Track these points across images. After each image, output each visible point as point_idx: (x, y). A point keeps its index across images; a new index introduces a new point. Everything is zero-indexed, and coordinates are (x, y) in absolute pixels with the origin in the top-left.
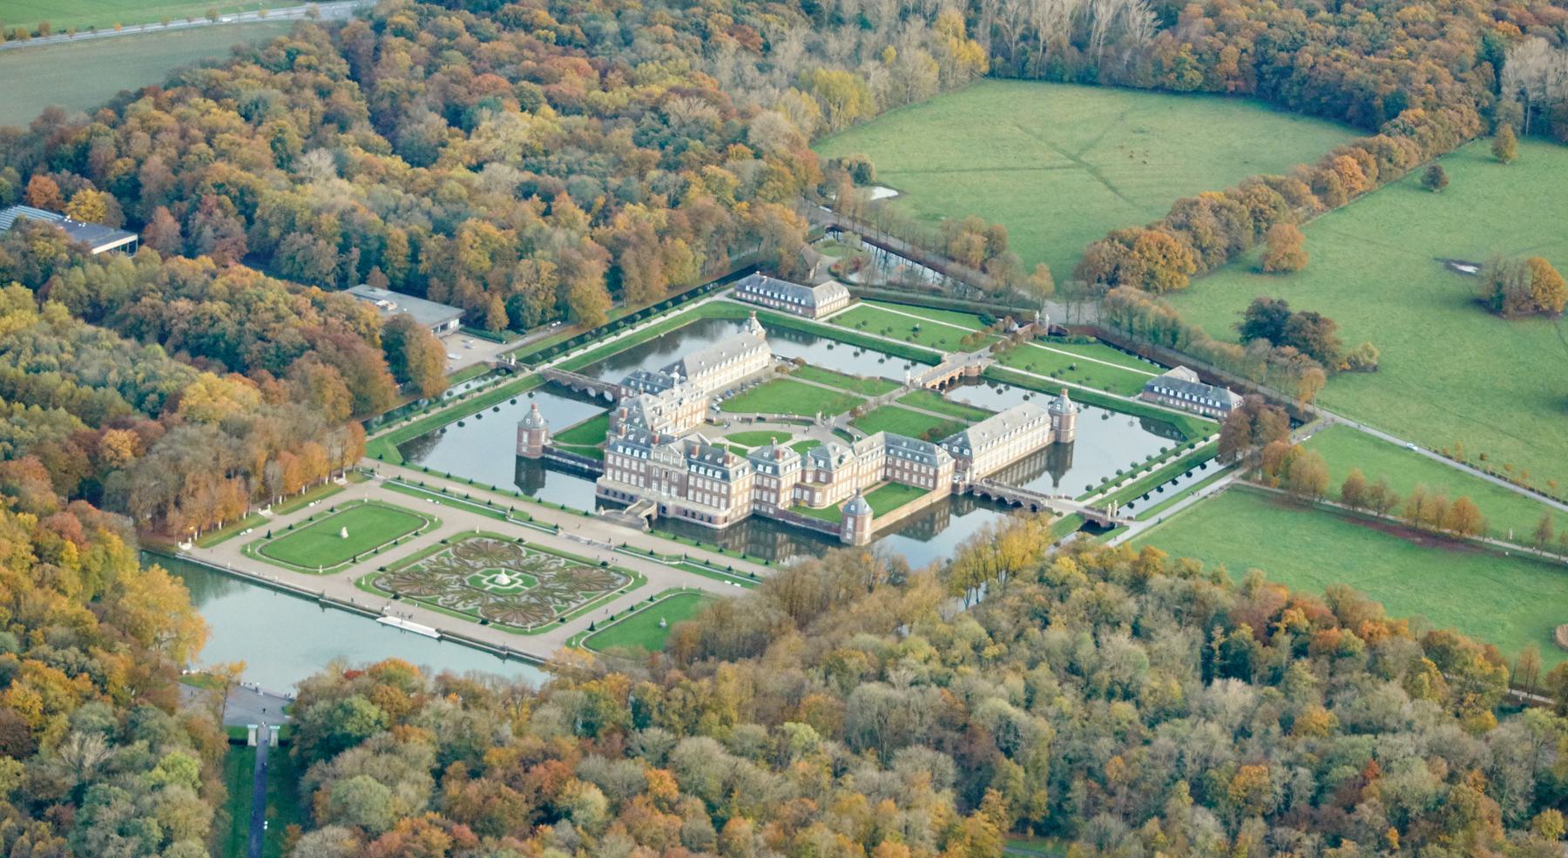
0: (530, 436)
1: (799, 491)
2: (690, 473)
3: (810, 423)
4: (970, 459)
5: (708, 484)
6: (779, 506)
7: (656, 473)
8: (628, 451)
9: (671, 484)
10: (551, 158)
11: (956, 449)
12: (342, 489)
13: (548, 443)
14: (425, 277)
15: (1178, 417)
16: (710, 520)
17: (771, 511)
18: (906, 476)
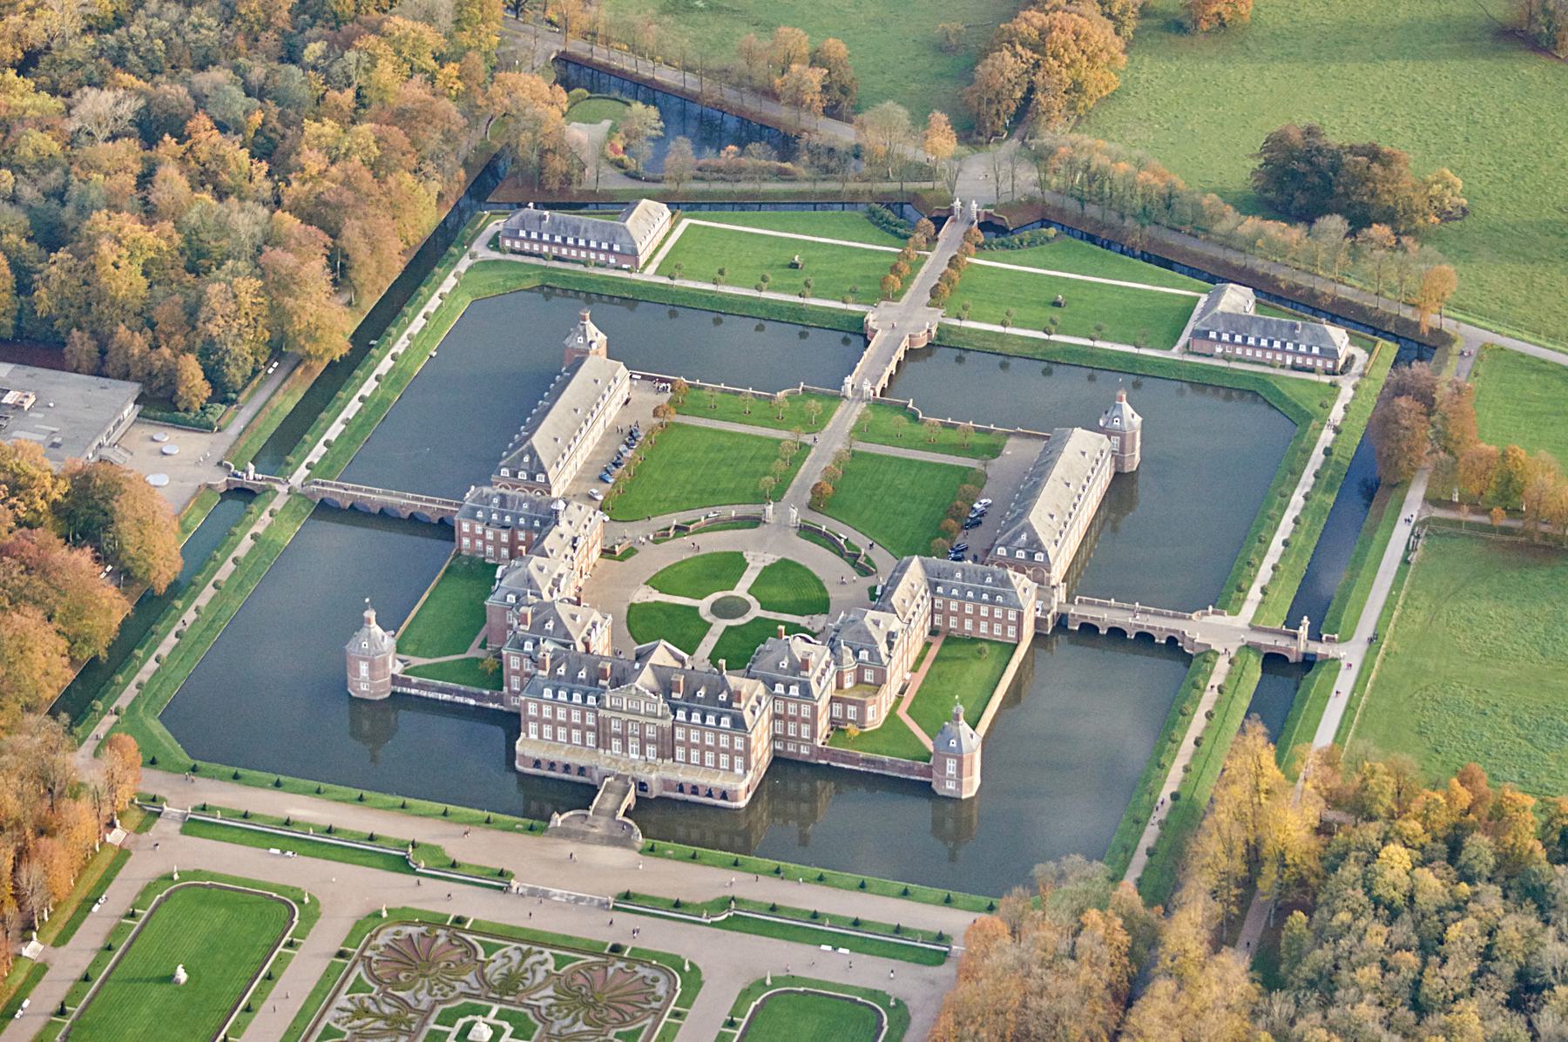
0: (372, 667)
1: (837, 707)
2: (675, 723)
3: (755, 522)
4: (1047, 565)
5: (709, 736)
6: (819, 744)
7: (615, 726)
8: (562, 696)
9: (644, 742)
10: (133, 29)
11: (1021, 554)
12: (123, 854)
13: (398, 669)
14: (49, 320)
15: (1259, 379)
16: (724, 796)
17: (804, 751)
18: (968, 624)
